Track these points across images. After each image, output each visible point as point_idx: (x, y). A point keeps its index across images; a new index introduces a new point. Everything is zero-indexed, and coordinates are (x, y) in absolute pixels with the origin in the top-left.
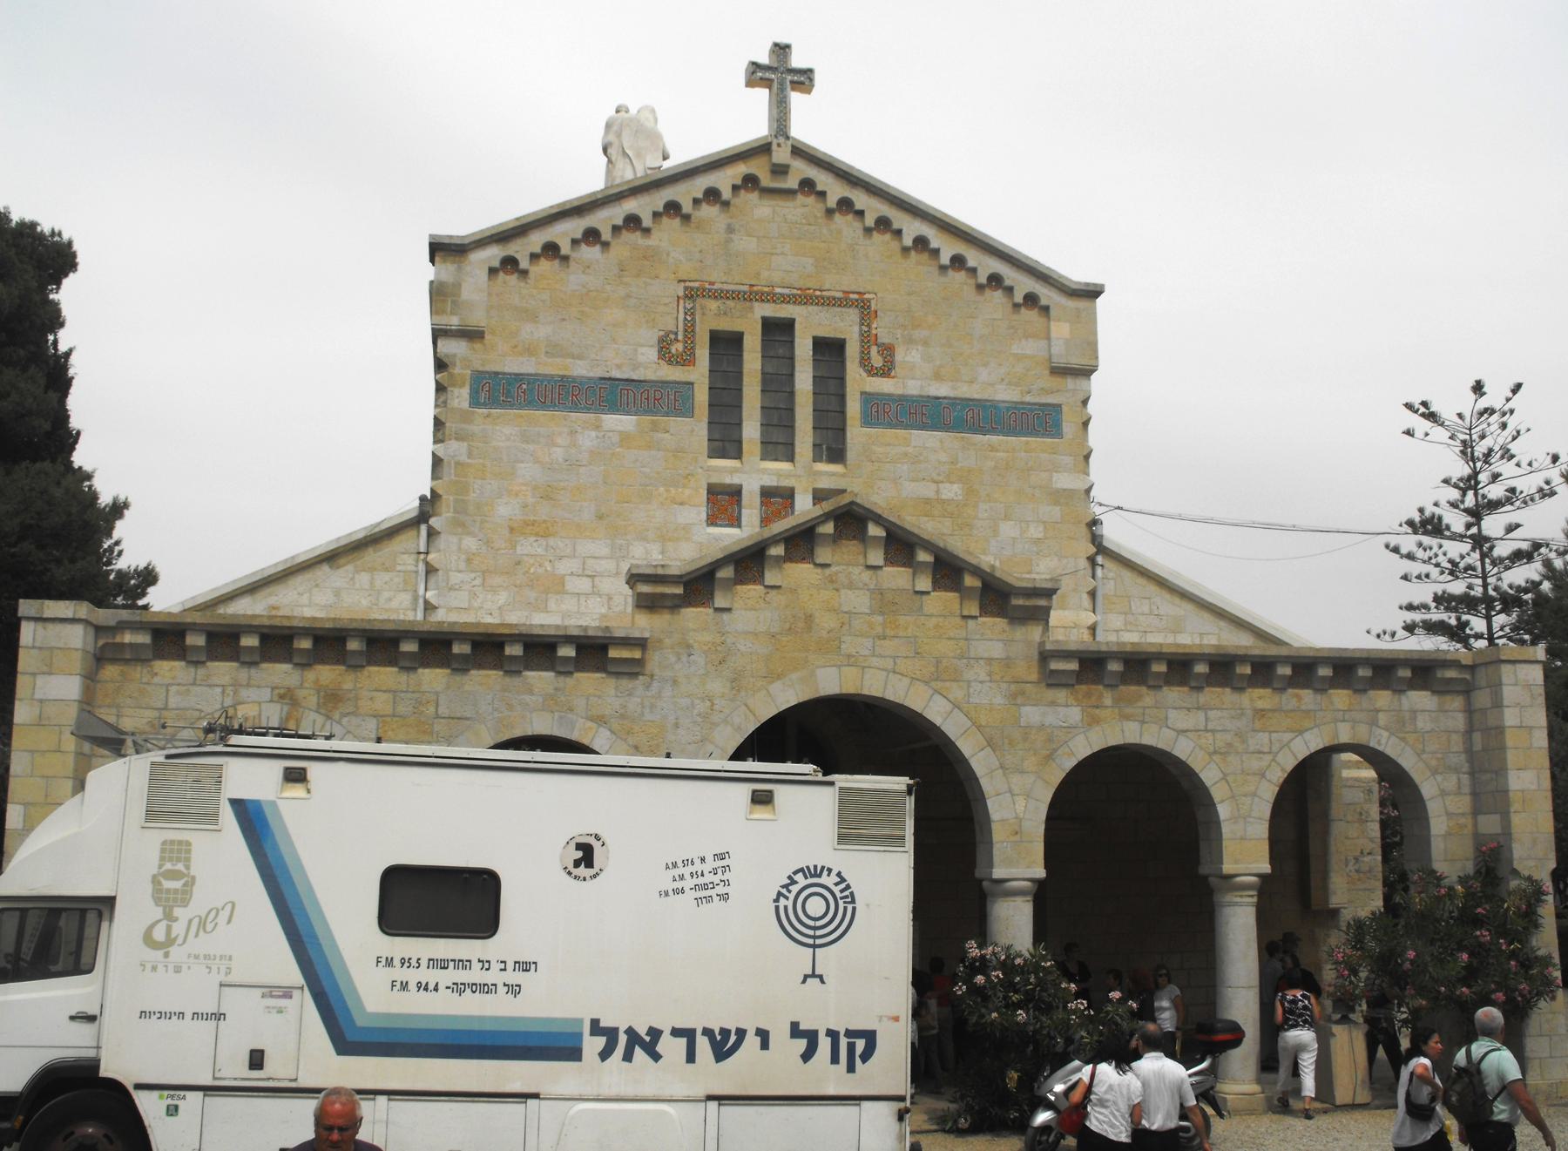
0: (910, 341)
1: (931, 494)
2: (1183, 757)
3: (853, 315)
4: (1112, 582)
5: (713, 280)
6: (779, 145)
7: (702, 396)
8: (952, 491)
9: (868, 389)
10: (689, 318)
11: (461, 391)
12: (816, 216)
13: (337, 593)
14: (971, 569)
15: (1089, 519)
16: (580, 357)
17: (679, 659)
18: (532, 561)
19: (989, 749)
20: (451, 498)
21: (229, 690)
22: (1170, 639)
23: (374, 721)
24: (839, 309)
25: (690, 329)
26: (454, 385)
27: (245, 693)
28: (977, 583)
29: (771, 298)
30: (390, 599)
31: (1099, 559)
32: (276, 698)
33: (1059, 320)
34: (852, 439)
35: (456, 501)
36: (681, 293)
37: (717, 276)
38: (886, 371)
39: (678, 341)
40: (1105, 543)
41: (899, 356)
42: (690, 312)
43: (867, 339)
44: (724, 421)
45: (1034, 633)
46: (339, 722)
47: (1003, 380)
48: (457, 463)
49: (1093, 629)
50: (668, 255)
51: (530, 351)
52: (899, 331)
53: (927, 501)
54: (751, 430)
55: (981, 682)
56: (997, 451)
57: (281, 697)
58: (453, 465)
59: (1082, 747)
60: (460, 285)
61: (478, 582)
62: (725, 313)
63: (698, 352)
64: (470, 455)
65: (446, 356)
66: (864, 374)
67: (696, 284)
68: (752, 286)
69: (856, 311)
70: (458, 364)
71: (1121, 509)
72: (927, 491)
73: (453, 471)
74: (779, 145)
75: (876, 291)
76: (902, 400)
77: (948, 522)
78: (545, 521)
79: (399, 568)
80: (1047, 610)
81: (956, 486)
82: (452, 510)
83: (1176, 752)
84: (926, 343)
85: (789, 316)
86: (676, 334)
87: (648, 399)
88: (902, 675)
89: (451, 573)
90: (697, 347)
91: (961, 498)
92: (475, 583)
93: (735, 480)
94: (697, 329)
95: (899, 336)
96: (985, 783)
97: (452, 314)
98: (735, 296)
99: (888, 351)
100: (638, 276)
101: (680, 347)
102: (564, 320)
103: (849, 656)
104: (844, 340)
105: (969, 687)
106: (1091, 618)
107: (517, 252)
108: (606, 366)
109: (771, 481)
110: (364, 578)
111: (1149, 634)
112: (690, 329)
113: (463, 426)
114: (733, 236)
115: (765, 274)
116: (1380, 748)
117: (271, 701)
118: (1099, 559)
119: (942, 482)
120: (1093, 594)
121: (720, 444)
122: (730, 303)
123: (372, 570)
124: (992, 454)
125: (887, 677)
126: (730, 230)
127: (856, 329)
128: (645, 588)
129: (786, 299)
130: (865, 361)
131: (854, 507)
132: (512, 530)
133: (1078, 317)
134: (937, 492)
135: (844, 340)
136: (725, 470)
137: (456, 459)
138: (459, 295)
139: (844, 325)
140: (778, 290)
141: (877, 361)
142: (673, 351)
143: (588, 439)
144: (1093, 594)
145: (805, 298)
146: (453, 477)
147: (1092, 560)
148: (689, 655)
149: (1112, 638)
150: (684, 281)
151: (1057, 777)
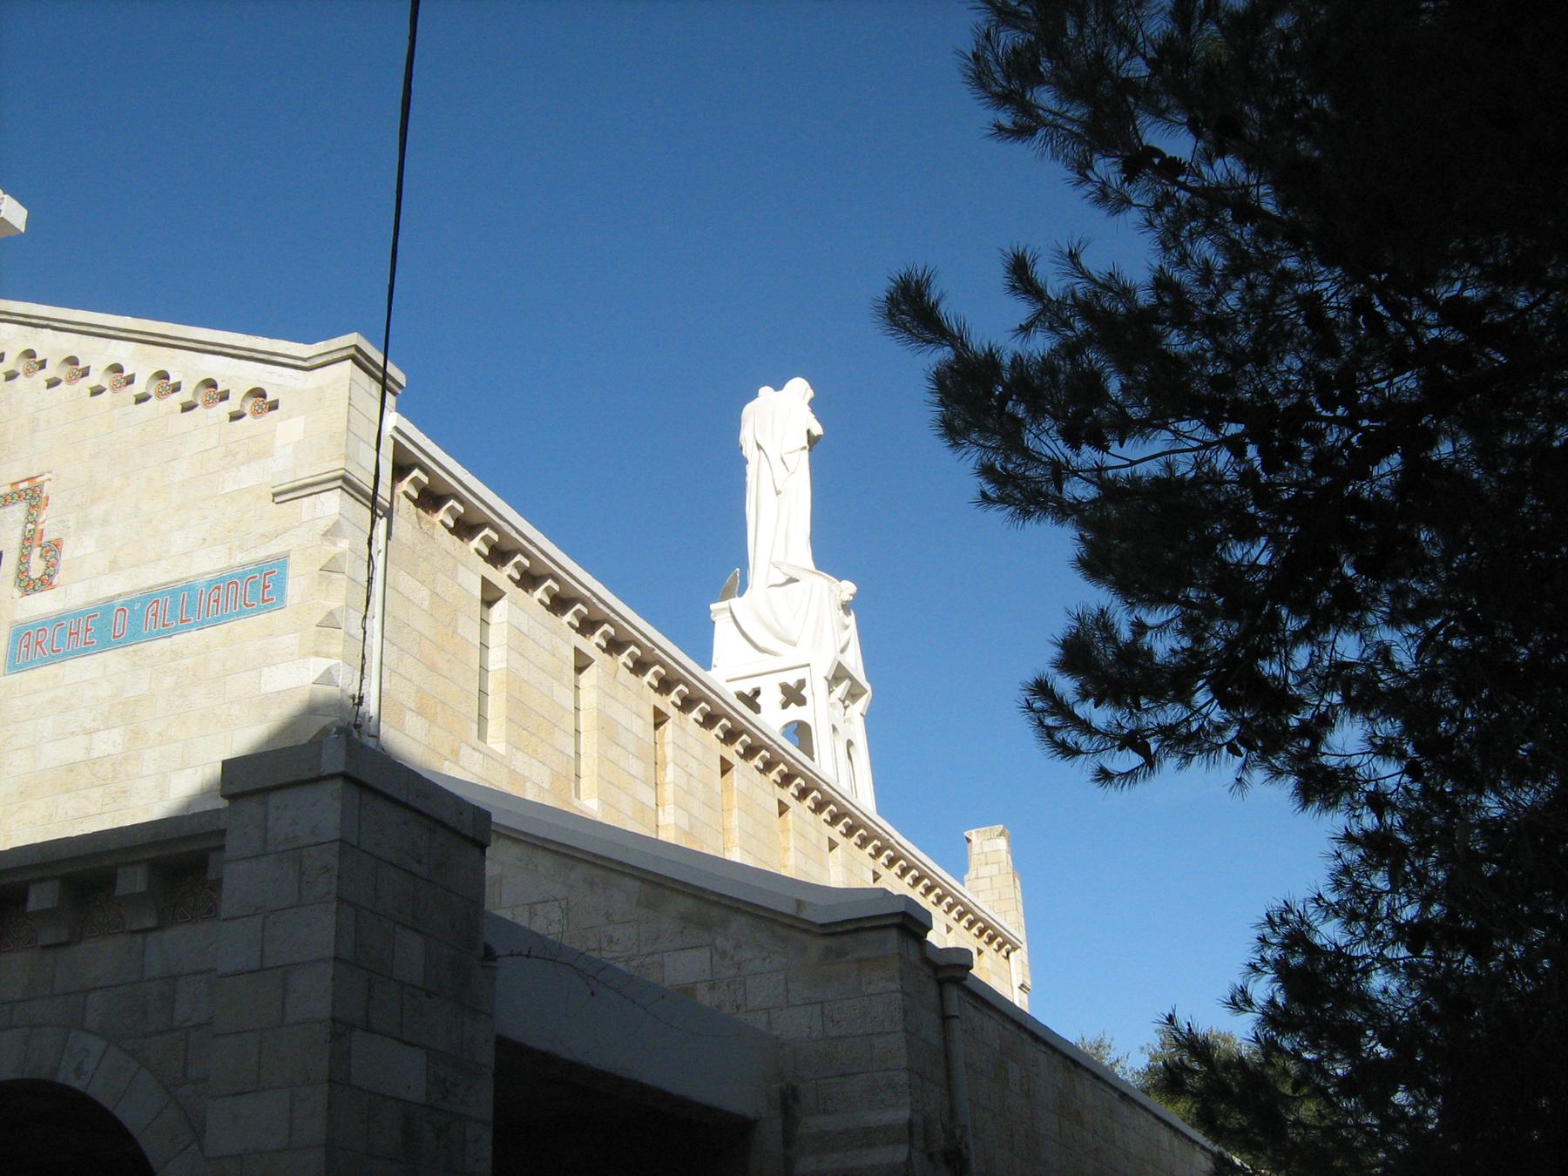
8: (108, 743)
33: (290, 417)
41: (66, 554)
43: (28, 541)
53: (71, 767)
66: (17, 593)
76: (59, 621)
81: (115, 731)
99: (53, 550)
116: (78, 1084)
133: (320, 400)
134: (89, 749)
141: (37, 567)
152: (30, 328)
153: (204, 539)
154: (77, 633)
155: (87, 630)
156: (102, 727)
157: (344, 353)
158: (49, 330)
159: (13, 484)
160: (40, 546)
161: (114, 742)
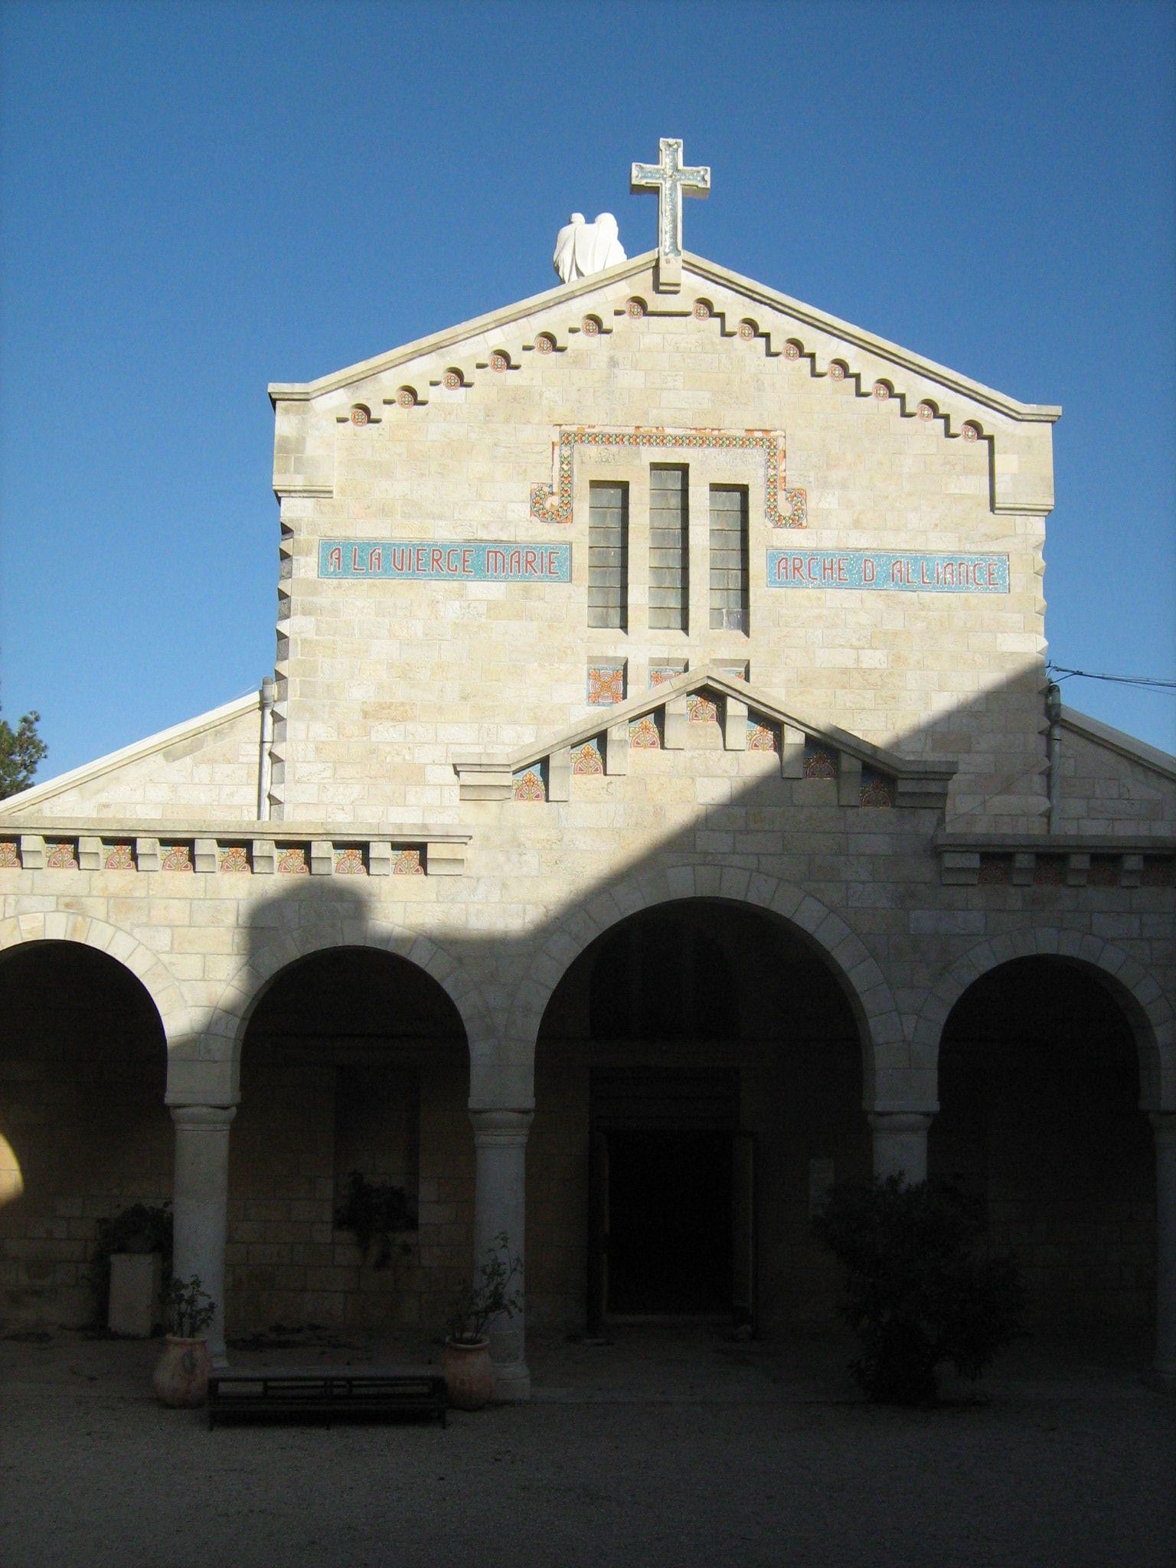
0: (824, 485)
1: (851, 664)
2: (1111, 970)
3: (758, 455)
4: (1073, 760)
5: (594, 424)
6: (668, 262)
7: (582, 558)
8: (874, 659)
9: (776, 543)
10: (566, 468)
11: (308, 559)
12: (713, 343)
13: (174, 788)
14: (849, 751)
15: (1045, 685)
16: (440, 517)
17: (509, 860)
18: (388, 749)
19: (871, 960)
20: (298, 680)
21: (11, 899)
22: (1143, 830)
23: (168, 930)
24: (740, 451)
25: (567, 478)
26: (299, 554)
27: (27, 902)
28: (857, 766)
29: (659, 440)
30: (232, 794)
31: (1057, 732)
32: (62, 907)
33: (1005, 452)
34: (756, 601)
35: (303, 682)
36: (556, 438)
37: (599, 420)
38: (796, 521)
39: (552, 494)
40: (1064, 716)
41: (812, 503)
42: (566, 461)
43: (771, 483)
44: (608, 585)
45: (926, 822)
46: (131, 934)
47: (937, 525)
48: (305, 641)
49: (1048, 815)
50: (541, 395)
51: (385, 511)
52: (812, 474)
53: (845, 671)
54: (639, 595)
55: (863, 882)
56: (929, 610)
57: (67, 906)
58: (299, 643)
59: (984, 959)
60: (304, 439)
61: (328, 773)
62: (607, 461)
63: (576, 506)
64: (318, 632)
65: (292, 521)
66: (770, 525)
67: (574, 428)
68: (638, 427)
69: (761, 451)
70: (304, 529)
71: (1081, 674)
72: (846, 658)
73: (299, 649)
74: (668, 262)
75: (784, 427)
76: (813, 555)
77: (870, 694)
78: (402, 704)
79: (242, 759)
80: (943, 795)
81: (878, 653)
82: (299, 695)
83: (1102, 964)
84: (844, 486)
85: (682, 462)
86: (551, 486)
87: (518, 562)
88: (768, 875)
89: (298, 765)
90: (575, 501)
91: (885, 666)
92: (324, 775)
93: (621, 653)
94: (575, 480)
95: (812, 479)
96: (868, 1002)
97: (297, 472)
98: (620, 439)
99: (797, 496)
100: (507, 421)
101: (554, 501)
102: (423, 475)
103: (706, 853)
104: (747, 486)
105: (847, 889)
106: (1043, 804)
107: (368, 399)
108: (471, 526)
109: (661, 653)
110: (204, 772)
111: (1117, 824)
112: (567, 478)
113: (310, 598)
114: (616, 370)
115: (654, 412)
117: (57, 911)
118: (1057, 732)
119: (864, 648)
120: (1048, 774)
121: (605, 610)
122: (614, 449)
123: (212, 761)
124: (923, 613)
125: (750, 877)
126: (613, 363)
127: (761, 472)
128: (467, 778)
129: (678, 441)
130: (772, 511)
131: (711, 683)
132: (366, 714)
134: (858, 660)
135: (747, 486)
136: (611, 644)
137: (303, 636)
138: (302, 451)
139: (749, 469)
140: (668, 431)
141: (785, 508)
142: (547, 506)
143: (452, 610)
144: (1048, 774)
145: (701, 440)
146: (299, 657)
147: (1048, 735)
148: (520, 855)
149: (1071, 829)
150: (560, 425)
151: (952, 992)
152: (748, 300)
153: (937, 525)
154: (832, 569)
155: (840, 569)
156: (866, 647)
157: (1050, 419)
158: (767, 307)
159: (747, 430)
160: (785, 490)
161: (880, 660)
